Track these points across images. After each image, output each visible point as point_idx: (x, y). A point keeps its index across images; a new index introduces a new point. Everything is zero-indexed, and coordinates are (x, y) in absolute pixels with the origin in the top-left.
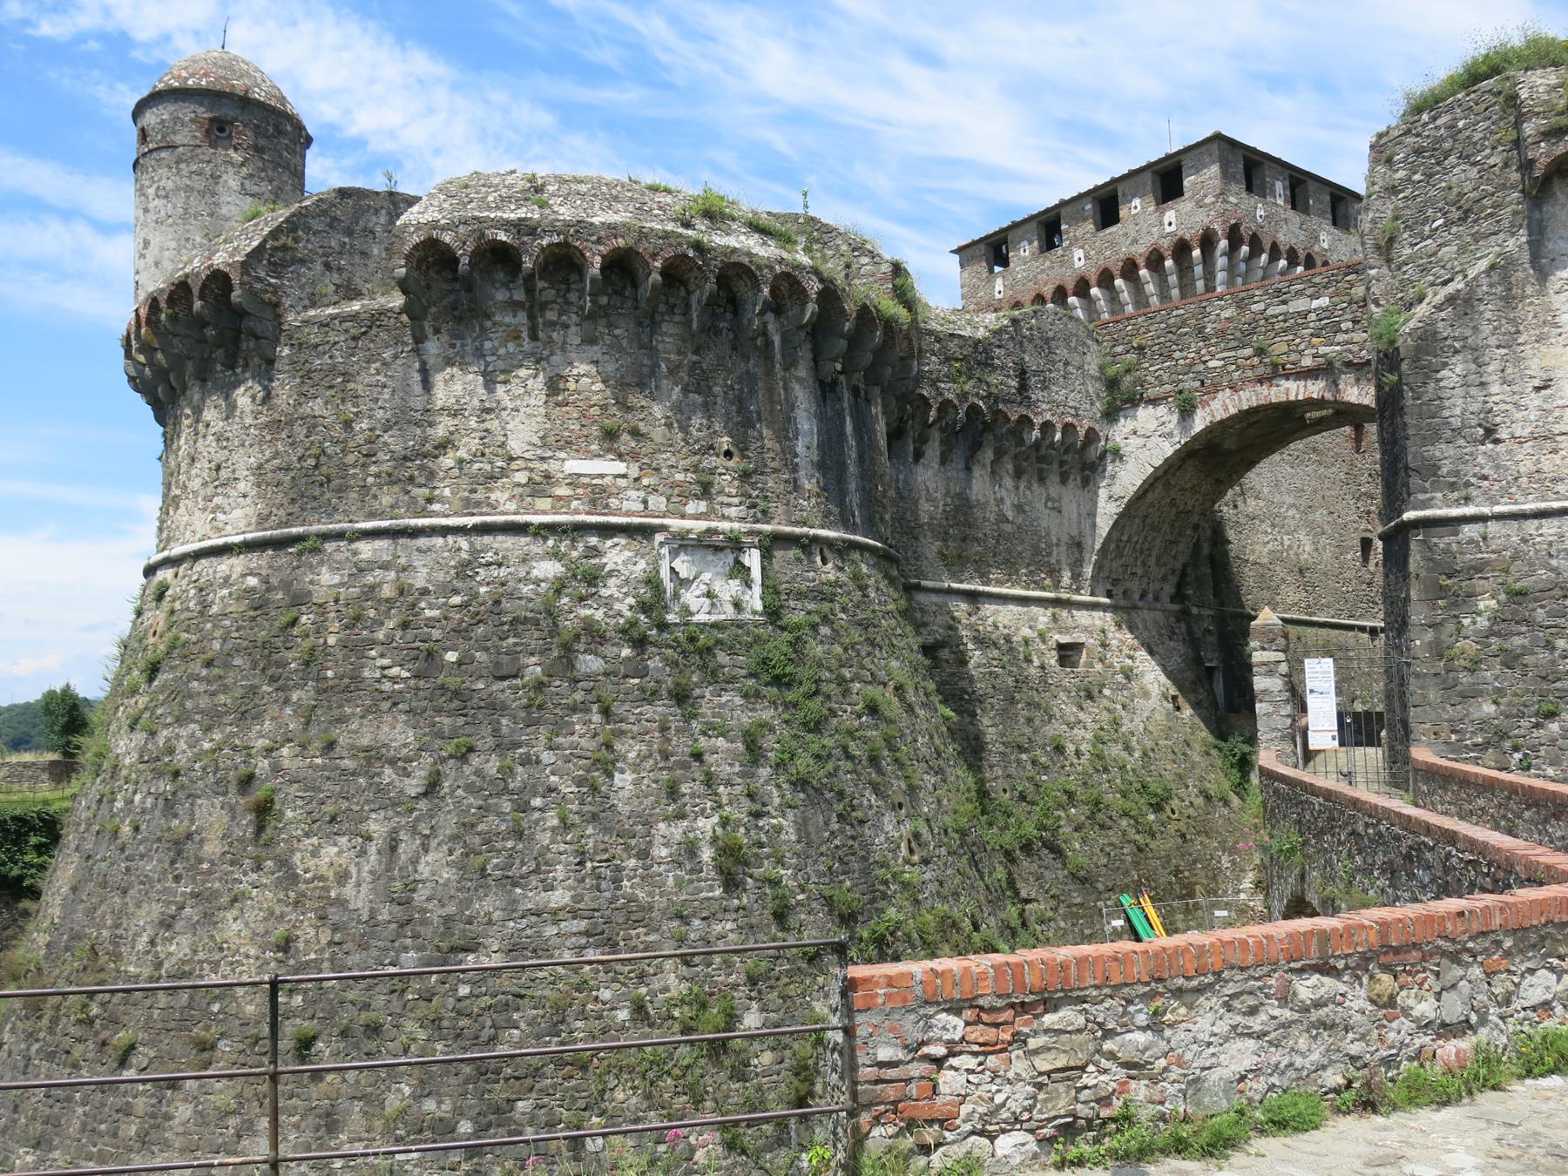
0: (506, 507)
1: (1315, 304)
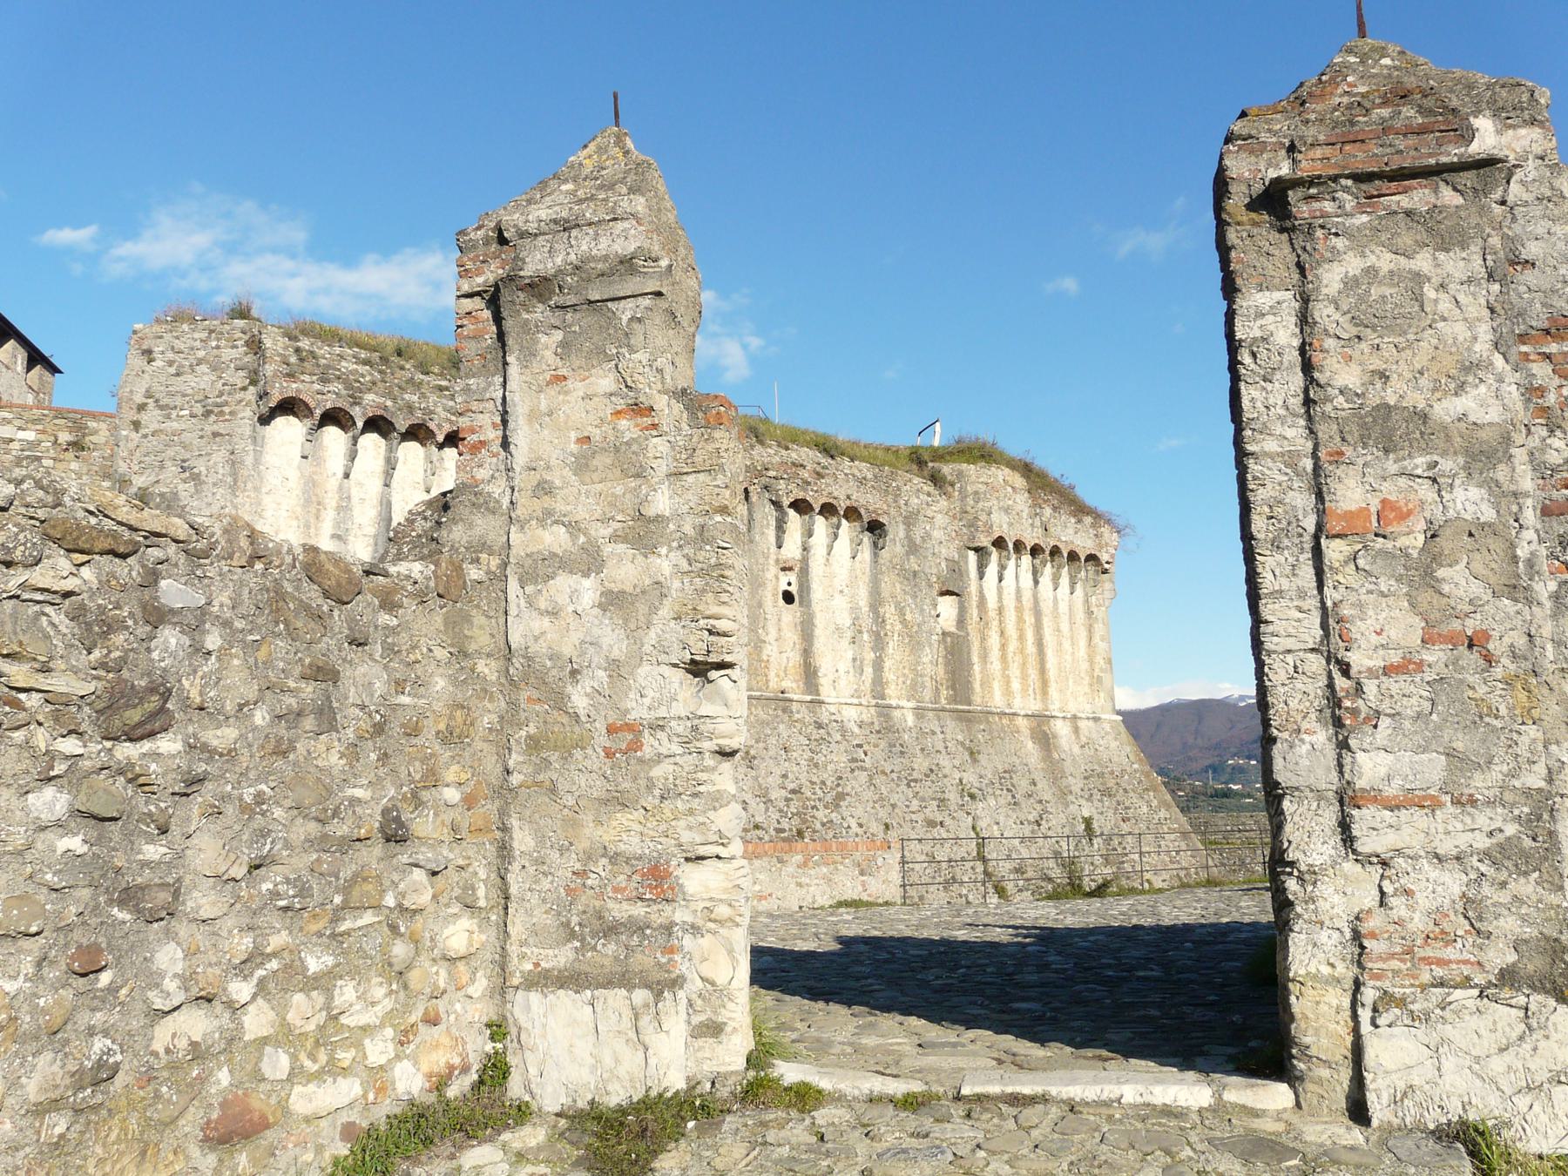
1: (21, 435)
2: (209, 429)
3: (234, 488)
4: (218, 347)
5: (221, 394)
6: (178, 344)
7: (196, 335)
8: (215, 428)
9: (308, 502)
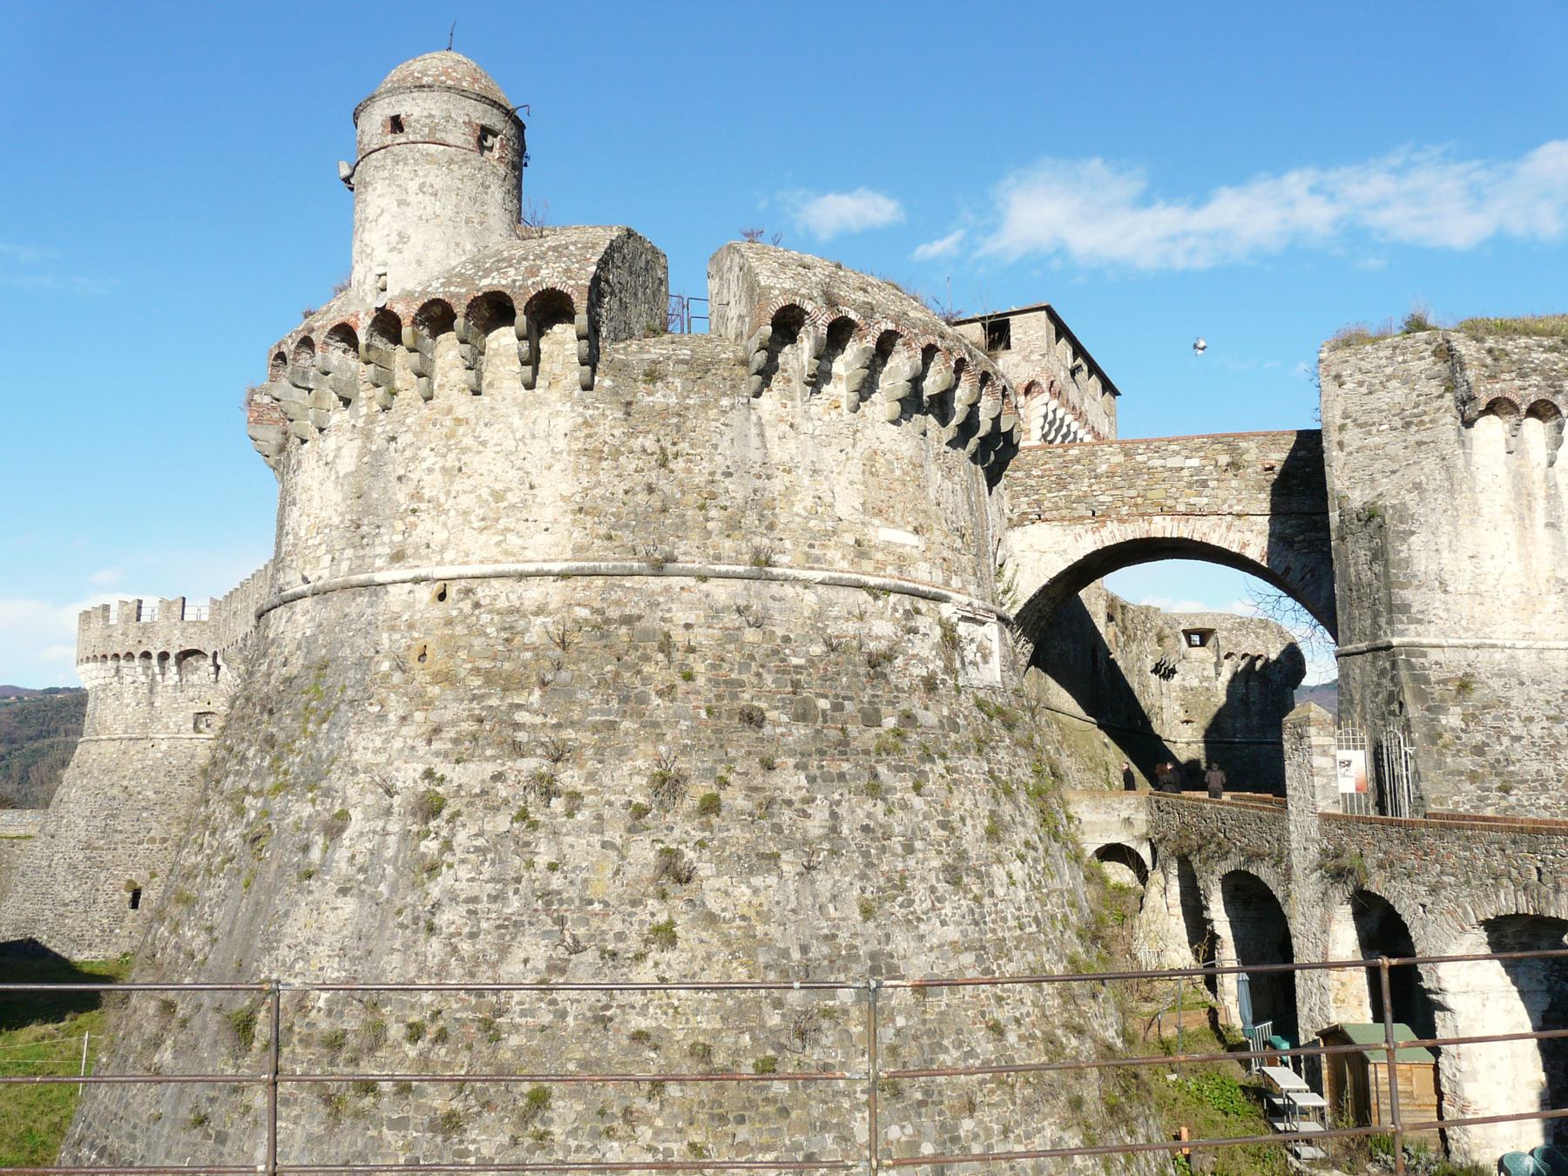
0: (842, 567)
1: (1189, 463)
2: (1412, 439)
3: (1451, 491)
4: (1405, 362)
5: (1417, 405)
6: (1365, 365)
7: (1381, 354)
8: (1418, 437)
9: (1518, 496)
